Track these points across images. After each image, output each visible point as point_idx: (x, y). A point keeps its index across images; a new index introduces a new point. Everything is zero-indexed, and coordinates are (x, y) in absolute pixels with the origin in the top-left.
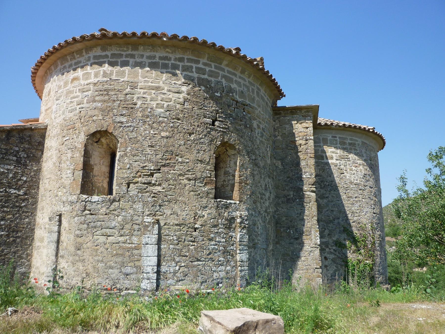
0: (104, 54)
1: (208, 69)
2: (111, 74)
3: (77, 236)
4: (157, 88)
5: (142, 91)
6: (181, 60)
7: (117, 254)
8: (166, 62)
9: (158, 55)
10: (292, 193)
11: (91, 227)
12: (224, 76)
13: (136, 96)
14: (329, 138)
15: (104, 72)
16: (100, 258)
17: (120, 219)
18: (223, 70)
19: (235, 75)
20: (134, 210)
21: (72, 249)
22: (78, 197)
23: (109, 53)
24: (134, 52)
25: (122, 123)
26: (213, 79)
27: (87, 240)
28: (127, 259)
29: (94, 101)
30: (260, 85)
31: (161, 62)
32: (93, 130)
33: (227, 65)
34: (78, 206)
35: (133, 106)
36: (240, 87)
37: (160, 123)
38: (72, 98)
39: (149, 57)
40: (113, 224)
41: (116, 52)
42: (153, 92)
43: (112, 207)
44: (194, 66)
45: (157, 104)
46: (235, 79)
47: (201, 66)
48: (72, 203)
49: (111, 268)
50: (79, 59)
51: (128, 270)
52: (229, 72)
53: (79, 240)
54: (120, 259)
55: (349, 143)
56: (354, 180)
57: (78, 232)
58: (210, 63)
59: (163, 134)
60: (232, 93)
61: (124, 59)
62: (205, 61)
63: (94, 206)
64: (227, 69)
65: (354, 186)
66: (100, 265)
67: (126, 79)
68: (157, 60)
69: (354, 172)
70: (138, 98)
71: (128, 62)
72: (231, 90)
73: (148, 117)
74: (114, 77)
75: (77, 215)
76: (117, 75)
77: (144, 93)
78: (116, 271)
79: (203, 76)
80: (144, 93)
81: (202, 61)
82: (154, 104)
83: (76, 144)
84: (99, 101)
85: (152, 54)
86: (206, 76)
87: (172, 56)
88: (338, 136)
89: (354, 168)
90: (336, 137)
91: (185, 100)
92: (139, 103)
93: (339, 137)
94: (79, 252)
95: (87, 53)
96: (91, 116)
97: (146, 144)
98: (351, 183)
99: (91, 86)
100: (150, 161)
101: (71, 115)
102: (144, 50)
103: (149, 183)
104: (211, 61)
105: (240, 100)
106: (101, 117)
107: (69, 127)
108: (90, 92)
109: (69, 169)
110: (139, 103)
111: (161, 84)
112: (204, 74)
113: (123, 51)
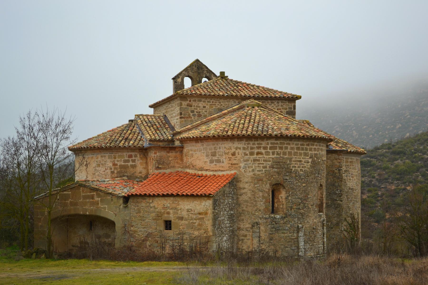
0: (276, 142)
2: (280, 154)
3: (270, 234)
4: (300, 161)
5: (294, 163)
7: (289, 242)
8: (303, 147)
9: (300, 143)
10: (330, 202)
11: (277, 230)
13: (292, 165)
15: (277, 152)
16: (282, 244)
17: (289, 226)
20: (295, 221)
21: (268, 240)
22: (269, 216)
23: (279, 142)
24: (290, 142)
25: (287, 180)
27: (276, 236)
28: (292, 243)
29: (273, 168)
31: (301, 147)
32: (274, 183)
34: (269, 220)
35: (291, 171)
37: (302, 179)
38: (258, 164)
39: (296, 145)
40: (287, 228)
41: (282, 142)
42: (299, 163)
43: (285, 220)
45: (301, 170)
48: (266, 218)
49: (287, 247)
50: (261, 142)
51: (293, 248)
53: (271, 236)
54: (290, 243)
57: (271, 232)
59: (304, 185)
61: (286, 145)
63: (277, 220)
66: (283, 246)
67: (287, 156)
68: (299, 146)
70: (293, 167)
71: (288, 147)
73: (297, 176)
74: (281, 156)
75: (270, 225)
76: (283, 155)
77: (295, 164)
78: (289, 249)
80: (295, 164)
82: (299, 169)
83: (265, 189)
84: (276, 168)
85: (298, 142)
87: (305, 143)
88: (344, 157)
89: (352, 178)
92: (293, 169)
93: (346, 158)
94: (272, 241)
95: (267, 140)
96: (272, 176)
97: (297, 190)
98: (350, 188)
99: (271, 159)
100: (299, 198)
101: (260, 173)
102: (294, 141)
103: (299, 209)
106: (277, 176)
107: (258, 179)
108: (271, 163)
109: (262, 202)
110: (293, 169)
111: (302, 159)
113: (286, 141)
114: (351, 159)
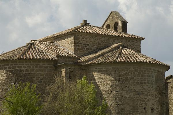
1: (12, 66)
6: (4, 66)
12: (18, 67)
14: (94, 70)
18: (18, 64)
19: (23, 64)
26: (14, 69)
30: (38, 62)
33: (19, 62)
36: (26, 68)
44: (7, 67)
46: (22, 66)
47: (10, 66)
52: (20, 64)
55: (104, 70)
56: (105, 89)
58: (12, 64)
60: (22, 72)
62: (11, 64)
64: (19, 63)
65: (105, 92)
69: (105, 85)
72: (21, 71)
79: (10, 69)
81: (10, 64)
86: (11, 69)
88: (98, 68)
89: (105, 83)
90: (97, 69)
91: (6, 79)
93: (99, 69)
104: (13, 63)
105: (24, 73)
112: (11, 69)
114: (105, 68)
